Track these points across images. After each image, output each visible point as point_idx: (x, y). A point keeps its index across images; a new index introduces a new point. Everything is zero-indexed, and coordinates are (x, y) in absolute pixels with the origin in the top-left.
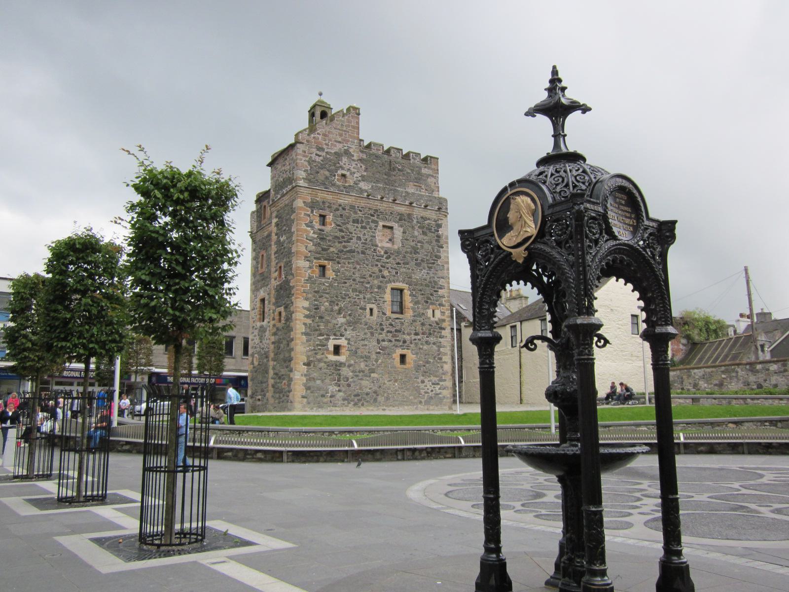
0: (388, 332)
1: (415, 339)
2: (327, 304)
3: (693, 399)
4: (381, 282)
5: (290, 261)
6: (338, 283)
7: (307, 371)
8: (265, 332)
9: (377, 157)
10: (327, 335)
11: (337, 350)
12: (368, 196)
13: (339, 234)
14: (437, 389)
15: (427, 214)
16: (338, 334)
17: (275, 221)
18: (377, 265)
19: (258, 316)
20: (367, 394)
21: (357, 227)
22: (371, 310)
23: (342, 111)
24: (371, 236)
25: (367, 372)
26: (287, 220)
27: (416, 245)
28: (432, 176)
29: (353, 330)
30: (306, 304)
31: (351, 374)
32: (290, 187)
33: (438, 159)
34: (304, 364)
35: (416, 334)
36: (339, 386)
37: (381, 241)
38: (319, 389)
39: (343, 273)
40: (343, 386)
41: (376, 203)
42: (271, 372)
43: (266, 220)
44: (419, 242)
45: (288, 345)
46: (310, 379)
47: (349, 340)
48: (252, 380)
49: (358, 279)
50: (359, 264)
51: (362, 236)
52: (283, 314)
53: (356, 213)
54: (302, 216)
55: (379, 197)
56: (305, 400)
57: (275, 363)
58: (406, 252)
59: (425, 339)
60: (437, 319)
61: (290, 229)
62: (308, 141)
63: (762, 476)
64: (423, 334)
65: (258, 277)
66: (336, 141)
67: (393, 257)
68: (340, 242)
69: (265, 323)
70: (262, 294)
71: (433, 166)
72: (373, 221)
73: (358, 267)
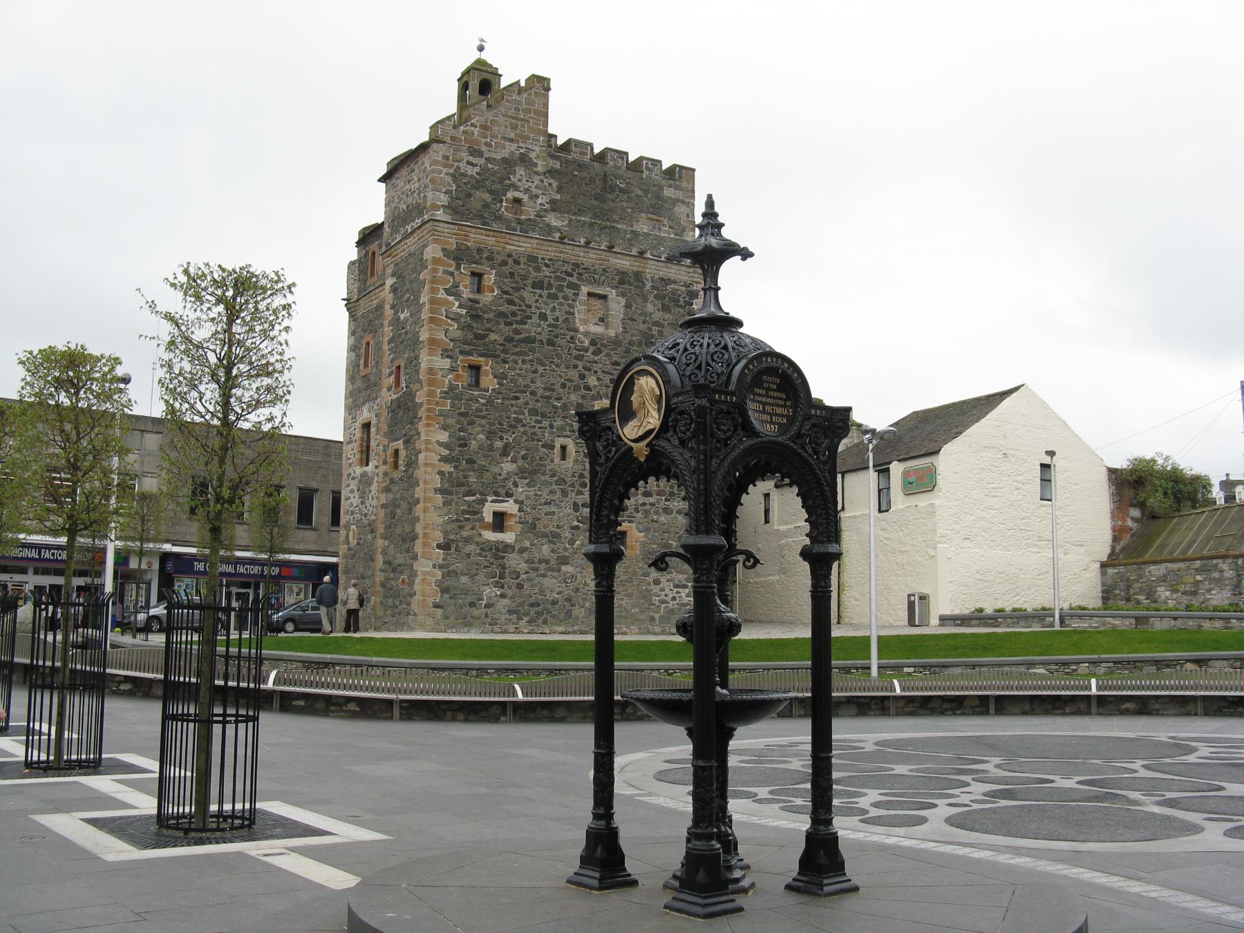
1: (644, 504)
2: (481, 436)
3: (1136, 618)
4: (583, 397)
5: (417, 357)
6: (504, 399)
8: (370, 484)
9: (581, 166)
10: (482, 494)
11: (500, 521)
12: (562, 238)
13: (506, 308)
14: (683, 595)
16: (502, 492)
17: (390, 281)
18: (575, 367)
19: (358, 456)
20: (554, 603)
21: (540, 296)
22: (563, 448)
23: (518, 83)
24: (567, 313)
25: (553, 562)
26: (412, 282)
27: (650, 329)
29: (528, 485)
30: (444, 437)
31: (524, 565)
32: (419, 221)
33: (694, 170)
34: (439, 546)
36: (503, 587)
37: (585, 322)
38: (465, 592)
39: (513, 381)
40: (510, 588)
41: (578, 251)
42: (380, 560)
43: (375, 278)
44: (656, 324)
45: (410, 510)
46: (449, 574)
47: (521, 503)
48: (347, 572)
49: (540, 392)
50: (544, 365)
52: (403, 454)
53: (538, 269)
54: (440, 274)
55: (583, 241)
56: (440, 611)
57: (387, 543)
58: (631, 343)
59: (663, 504)
61: (417, 298)
62: (453, 138)
63: (1192, 750)
64: (659, 494)
65: (359, 383)
66: (505, 139)
67: (605, 351)
68: (507, 324)
69: (369, 468)
70: (366, 414)
71: (684, 185)
73: (540, 369)
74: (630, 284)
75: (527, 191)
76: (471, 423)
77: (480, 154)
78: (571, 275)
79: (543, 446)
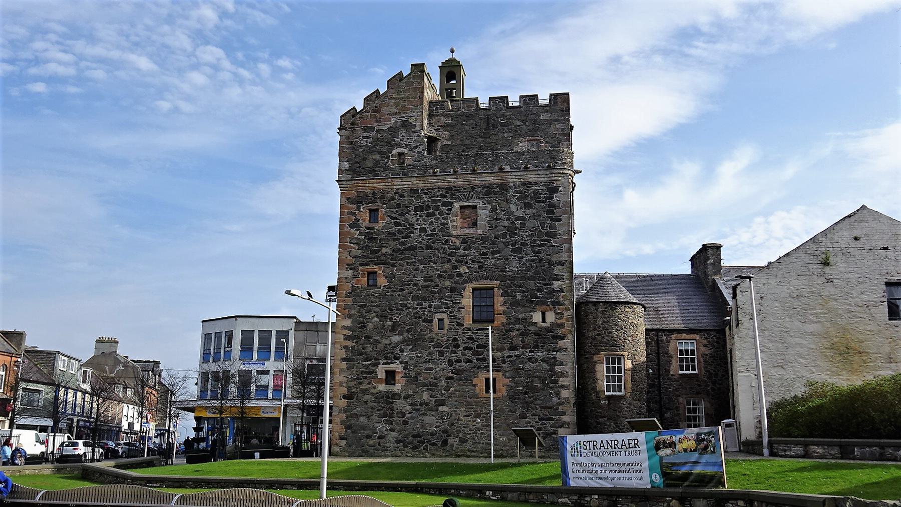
0: (465, 349)
1: (511, 356)
7: (348, 406)
10: (376, 359)
11: (391, 376)
13: (395, 229)
15: (532, 177)
18: (449, 261)
20: (432, 434)
21: (421, 216)
22: (441, 320)
25: (432, 404)
27: (513, 223)
28: (557, 120)
29: (412, 350)
30: (348, 322)
34: (345, 397)
35: (513, 348)
38: (364, 428)
40: (397, 424)
41: (449, 178)
44: (518, 219)
47: (406, 363)
49: (421, 283)
51: (427, 226)
55: (452, 171)
56: (344, 442)
58: (497, 237)
60: (547, 325)
66: (390, 114)
68: (394, 240)
72: (445, 204)
74: (495, 193)
75: (407, 146)
76: (369, 311)
77: (372, 129)
78: (446, 197)
79: (423, 321)
